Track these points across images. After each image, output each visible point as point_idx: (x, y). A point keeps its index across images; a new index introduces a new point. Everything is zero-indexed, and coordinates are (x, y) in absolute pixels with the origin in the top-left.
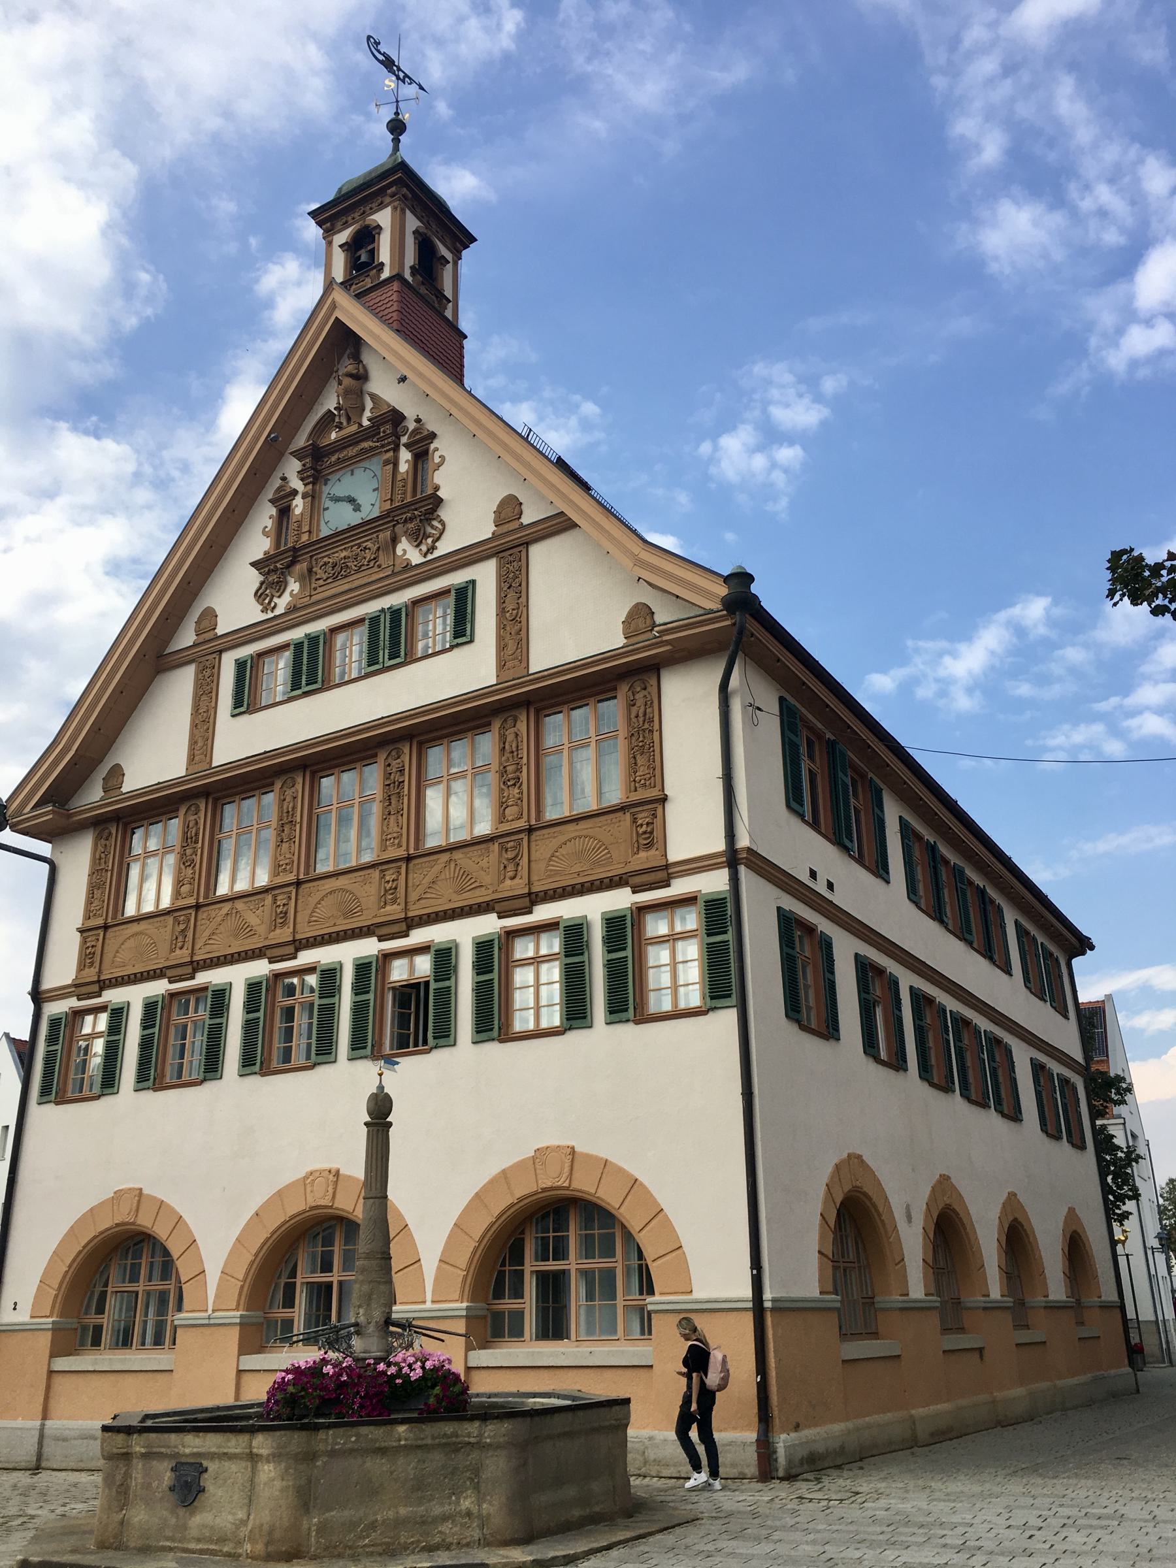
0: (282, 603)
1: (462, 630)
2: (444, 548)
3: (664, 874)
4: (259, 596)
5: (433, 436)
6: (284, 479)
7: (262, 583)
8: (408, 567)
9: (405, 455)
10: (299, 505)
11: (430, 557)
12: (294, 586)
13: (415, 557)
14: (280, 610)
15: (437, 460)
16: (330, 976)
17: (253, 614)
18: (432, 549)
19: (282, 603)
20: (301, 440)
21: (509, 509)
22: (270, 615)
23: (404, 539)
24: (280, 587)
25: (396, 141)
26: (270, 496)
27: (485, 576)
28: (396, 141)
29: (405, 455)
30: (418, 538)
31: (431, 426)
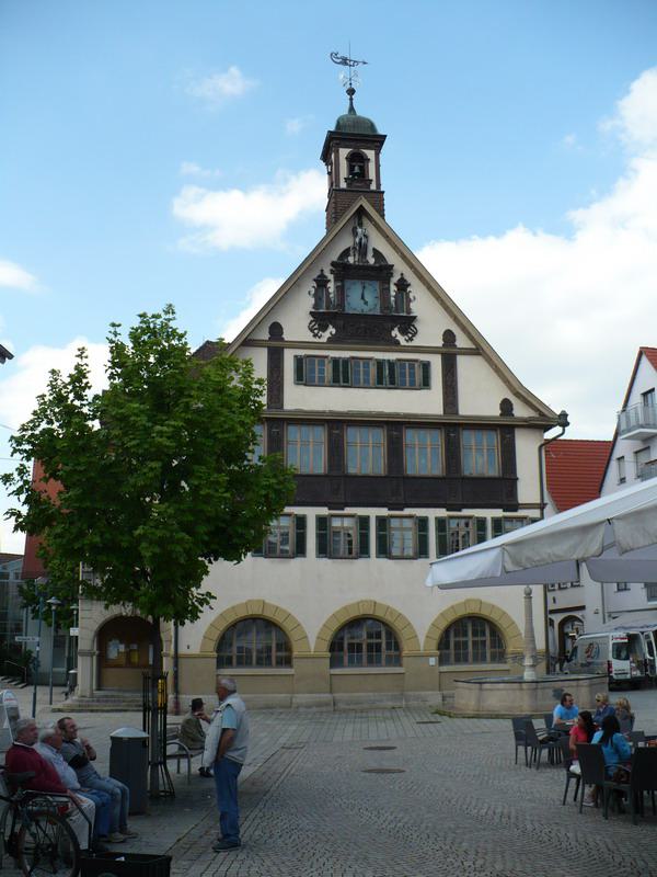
0: (326, 335)
1: (426, 384)
2: (417, 342)
3: (515, 507)
4: (312, 330)
5: (409, 285)
6: (322, 271)
7: (312, 322)
8: (398, 343)
9: (393, 288)
10: (331, 286)
11: (410, 344)
12: (331, 330)
13: (402, 339)
14: (324, 340)
15: (411, 296)
16: (364, 521)
17: (309, 337)
18: (411, 339)
19: (326, 335)
20: (334, 257)
21: (449, 337)
22: (317, 340)
23: (396, 329)
24: (324, 329)
25: (351, 99)
26: (315, 277)
27: (436, 363)
28: (351, 99)
29: (393, 288)
30: (404, 332)
31: (410, 277)
